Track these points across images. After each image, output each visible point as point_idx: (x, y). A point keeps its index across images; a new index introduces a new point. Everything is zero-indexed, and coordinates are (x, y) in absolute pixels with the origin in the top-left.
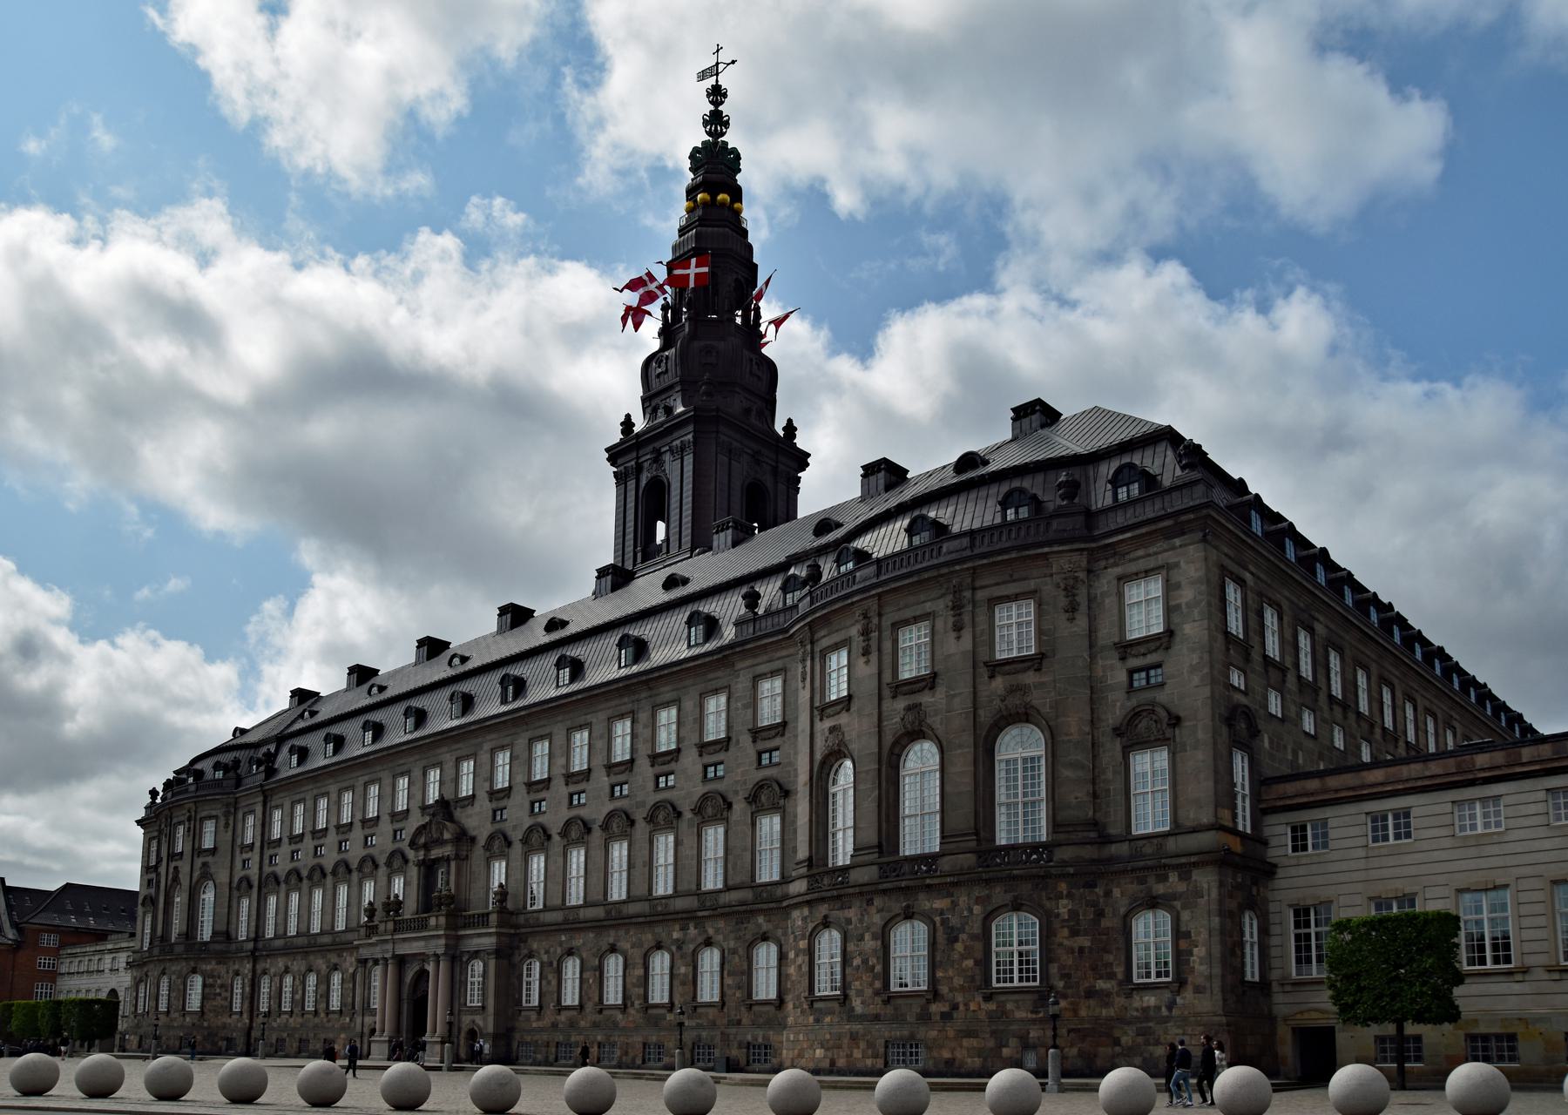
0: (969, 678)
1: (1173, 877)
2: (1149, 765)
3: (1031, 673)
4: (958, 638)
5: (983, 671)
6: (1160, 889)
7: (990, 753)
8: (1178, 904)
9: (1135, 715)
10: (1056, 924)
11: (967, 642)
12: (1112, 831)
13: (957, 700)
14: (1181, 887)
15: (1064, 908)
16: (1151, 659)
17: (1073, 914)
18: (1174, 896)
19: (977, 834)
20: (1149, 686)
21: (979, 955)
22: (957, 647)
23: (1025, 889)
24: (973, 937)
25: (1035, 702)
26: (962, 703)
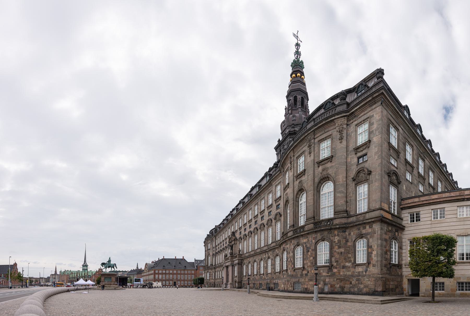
0: (312, 168)
1: (368, 227)
2: (363, 190)
3: (329, 163)
4: (310, 156)
5: (316, 165)
6: (364, 231)
7: (319, 192)
8: (369, 236)
9: (359, 172)
10: (334, 244)
11: (312, 157)
12: (352, 213)
13: (309, 176)
14: (370, 230)
15: (336, 239)
16: (364, 152)
17: (339, 241)
18: (367, 234)
19: (314, 218)
20: (363, 162)
21: (314, 256)
22: (310, 159)
23: (326, 233)
24: (312, 250)
25: (330, 173)
26: (311, 177)
